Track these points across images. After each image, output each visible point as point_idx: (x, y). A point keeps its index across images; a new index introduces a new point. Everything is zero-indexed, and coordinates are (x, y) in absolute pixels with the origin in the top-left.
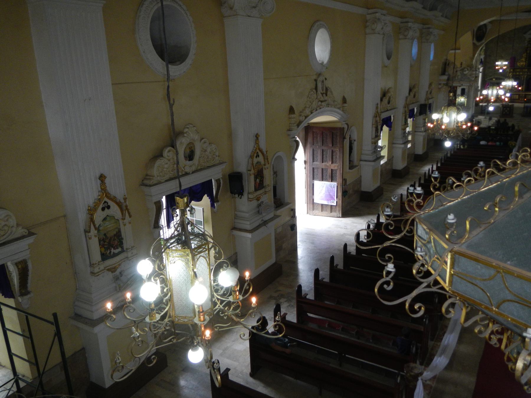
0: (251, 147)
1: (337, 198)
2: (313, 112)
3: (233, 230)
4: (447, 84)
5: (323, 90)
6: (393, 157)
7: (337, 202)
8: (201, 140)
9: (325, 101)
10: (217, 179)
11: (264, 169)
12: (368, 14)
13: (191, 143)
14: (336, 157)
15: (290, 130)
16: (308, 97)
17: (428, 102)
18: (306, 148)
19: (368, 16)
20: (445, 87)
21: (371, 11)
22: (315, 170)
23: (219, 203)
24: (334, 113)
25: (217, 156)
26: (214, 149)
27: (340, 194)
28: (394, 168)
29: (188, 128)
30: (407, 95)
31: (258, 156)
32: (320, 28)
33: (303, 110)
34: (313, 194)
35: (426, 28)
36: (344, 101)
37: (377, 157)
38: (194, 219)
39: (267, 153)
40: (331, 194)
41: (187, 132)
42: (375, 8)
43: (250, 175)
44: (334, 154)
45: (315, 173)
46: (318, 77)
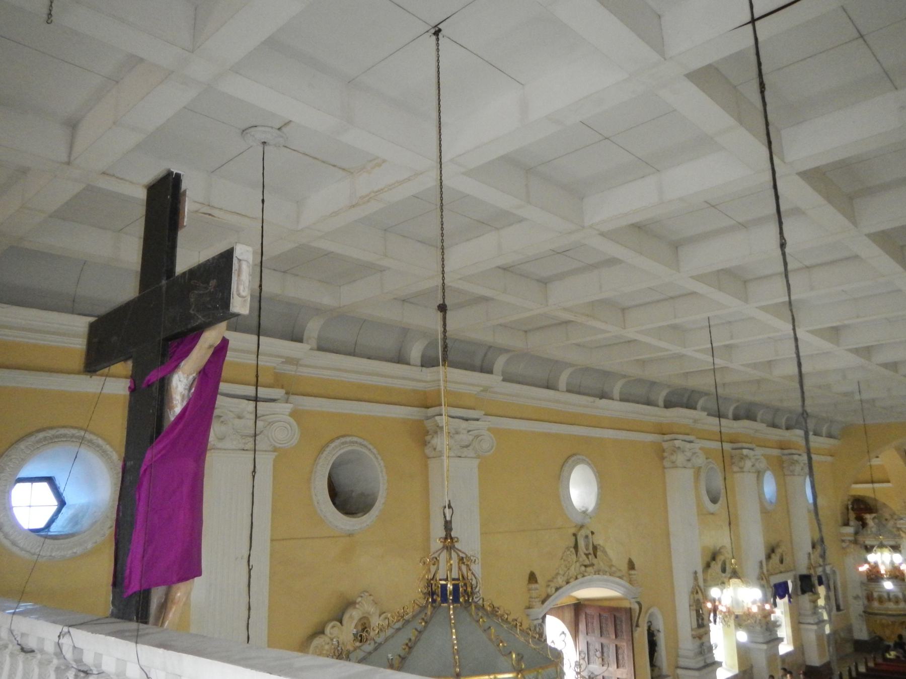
2: (571, 580)
4: (855, 542)
5: (587, 549)
6: (752, 667)
9: (592, 565)
12: (664, 441)
14: (623, 658)
15: (529, 608)
17: (815, 572)
19: (663, 443)
20: (852, 546)
21: (666, 437)
29: (362, 597)
30: (762, 556)
32: (577, 465)
33: (553, 578)
35: (787, 455)
36: (631, 566)
37: (705, 662)
41: (359, 602)
42: (670, 434)
44: (620, 651)
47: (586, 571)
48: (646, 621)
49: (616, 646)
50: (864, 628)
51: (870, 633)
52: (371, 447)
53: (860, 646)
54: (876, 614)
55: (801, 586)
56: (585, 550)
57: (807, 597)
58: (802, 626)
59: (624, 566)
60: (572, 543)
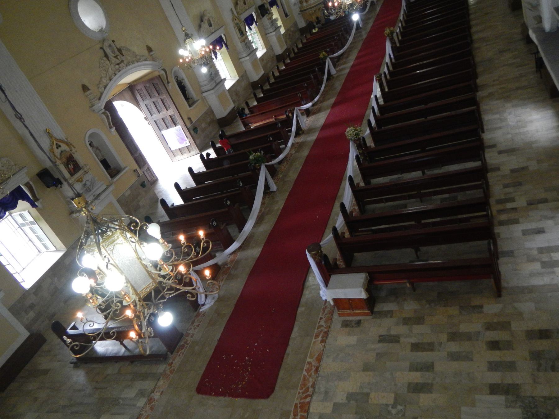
0: (45, 143)
1: (187, 138)
2: (113, 77)
3: (71, 215)
5: (114, 53)
7: (189, 141)
9: (122, 61)
10: (26, 182)
11: (72, 154)
16: (100, 67)
18: (139, 105)
22: (158, 122)
23: (41, 200)
24: (146, 66)
25: (13, 166)
26: (5, 162)
27: (188, 134)
28: (251, 81)
31: (58, 146)
33: (100, 81)
34: (168, 144)
36: (150, 50)
37: (216, 83)
39: (68, 141)
40: (181, 137)
44: (164, 101)
45: (159, 125)
46: (103, 44)
47: (120, 67)
48: (173, 78)
49: (161, 99)
50: (303, 20)
51: (306, 21)
53: (303, 31)
54: (306, 10)
55: (261, 13)
56: (114, 55)
57: (266, 18)
58: (268, 35)
59: (146, 52)
60: (101, 53)
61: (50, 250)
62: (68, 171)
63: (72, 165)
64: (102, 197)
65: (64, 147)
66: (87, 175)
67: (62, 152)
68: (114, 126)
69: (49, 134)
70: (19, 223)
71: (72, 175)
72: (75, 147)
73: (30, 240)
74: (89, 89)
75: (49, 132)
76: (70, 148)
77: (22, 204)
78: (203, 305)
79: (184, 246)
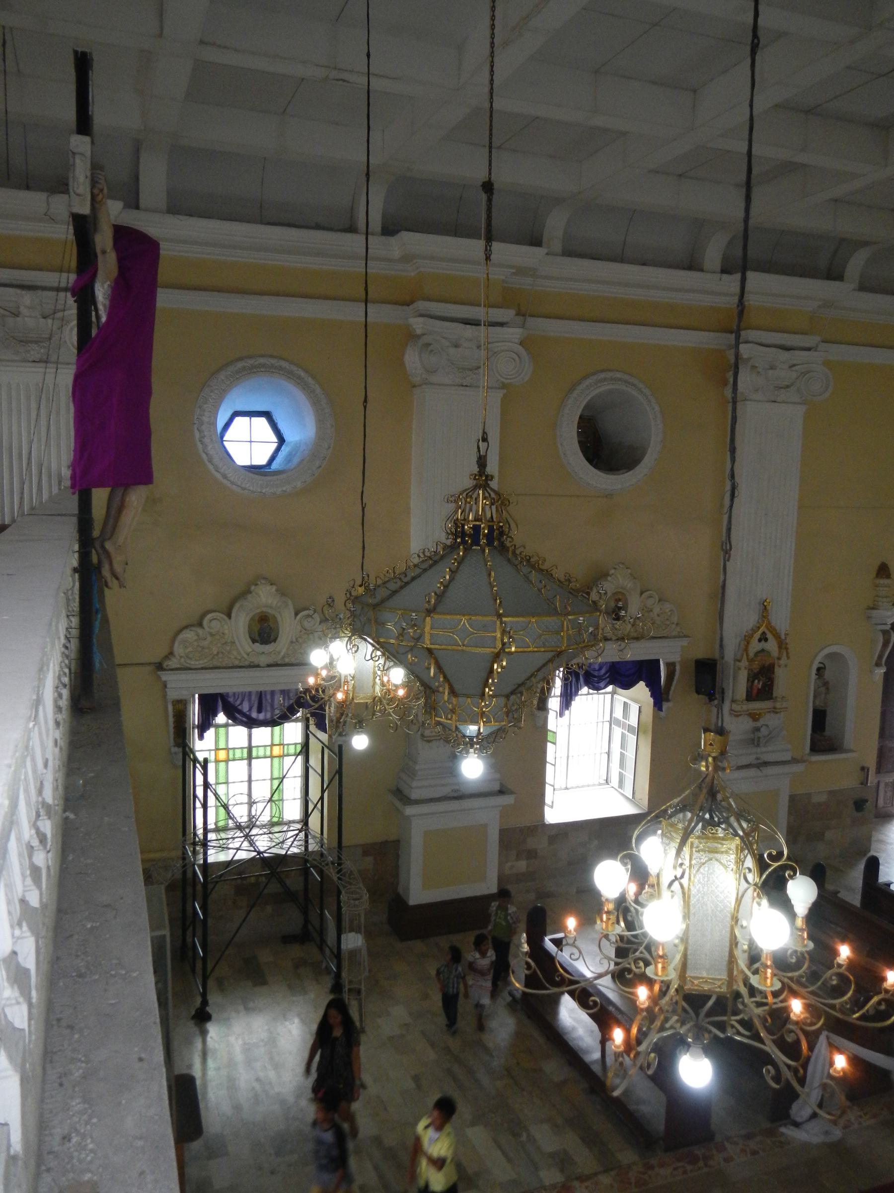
0: (751, 619)
8: (642, 593)
11: (776, 666)
13: (619, 592)
25: (673, 623)
26: (667, 611)
31: (763, 638)
38: (627, 722)
41: (613, 574)
43: (739, 669)
52: (641, 386)
61: (622, 791)
62: (747, 688)
63: (761, 683)
64: (771, 770)
65: (771, 646)
66: (772, 715)
67: (763, 650)
68: (886, 664)
69: (764, 610)
70: (614, 715)
71: (750, 698)
72: (788, 658)
73: (609, 754)
74: (888, 576)
75: (768, 608)
76: (780, 652)
77: (641, 690)
78: (797, 1125)
79: (835, 970)
